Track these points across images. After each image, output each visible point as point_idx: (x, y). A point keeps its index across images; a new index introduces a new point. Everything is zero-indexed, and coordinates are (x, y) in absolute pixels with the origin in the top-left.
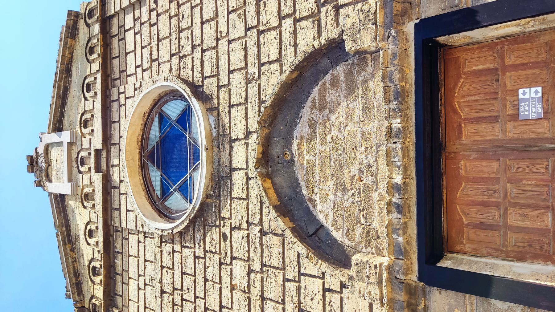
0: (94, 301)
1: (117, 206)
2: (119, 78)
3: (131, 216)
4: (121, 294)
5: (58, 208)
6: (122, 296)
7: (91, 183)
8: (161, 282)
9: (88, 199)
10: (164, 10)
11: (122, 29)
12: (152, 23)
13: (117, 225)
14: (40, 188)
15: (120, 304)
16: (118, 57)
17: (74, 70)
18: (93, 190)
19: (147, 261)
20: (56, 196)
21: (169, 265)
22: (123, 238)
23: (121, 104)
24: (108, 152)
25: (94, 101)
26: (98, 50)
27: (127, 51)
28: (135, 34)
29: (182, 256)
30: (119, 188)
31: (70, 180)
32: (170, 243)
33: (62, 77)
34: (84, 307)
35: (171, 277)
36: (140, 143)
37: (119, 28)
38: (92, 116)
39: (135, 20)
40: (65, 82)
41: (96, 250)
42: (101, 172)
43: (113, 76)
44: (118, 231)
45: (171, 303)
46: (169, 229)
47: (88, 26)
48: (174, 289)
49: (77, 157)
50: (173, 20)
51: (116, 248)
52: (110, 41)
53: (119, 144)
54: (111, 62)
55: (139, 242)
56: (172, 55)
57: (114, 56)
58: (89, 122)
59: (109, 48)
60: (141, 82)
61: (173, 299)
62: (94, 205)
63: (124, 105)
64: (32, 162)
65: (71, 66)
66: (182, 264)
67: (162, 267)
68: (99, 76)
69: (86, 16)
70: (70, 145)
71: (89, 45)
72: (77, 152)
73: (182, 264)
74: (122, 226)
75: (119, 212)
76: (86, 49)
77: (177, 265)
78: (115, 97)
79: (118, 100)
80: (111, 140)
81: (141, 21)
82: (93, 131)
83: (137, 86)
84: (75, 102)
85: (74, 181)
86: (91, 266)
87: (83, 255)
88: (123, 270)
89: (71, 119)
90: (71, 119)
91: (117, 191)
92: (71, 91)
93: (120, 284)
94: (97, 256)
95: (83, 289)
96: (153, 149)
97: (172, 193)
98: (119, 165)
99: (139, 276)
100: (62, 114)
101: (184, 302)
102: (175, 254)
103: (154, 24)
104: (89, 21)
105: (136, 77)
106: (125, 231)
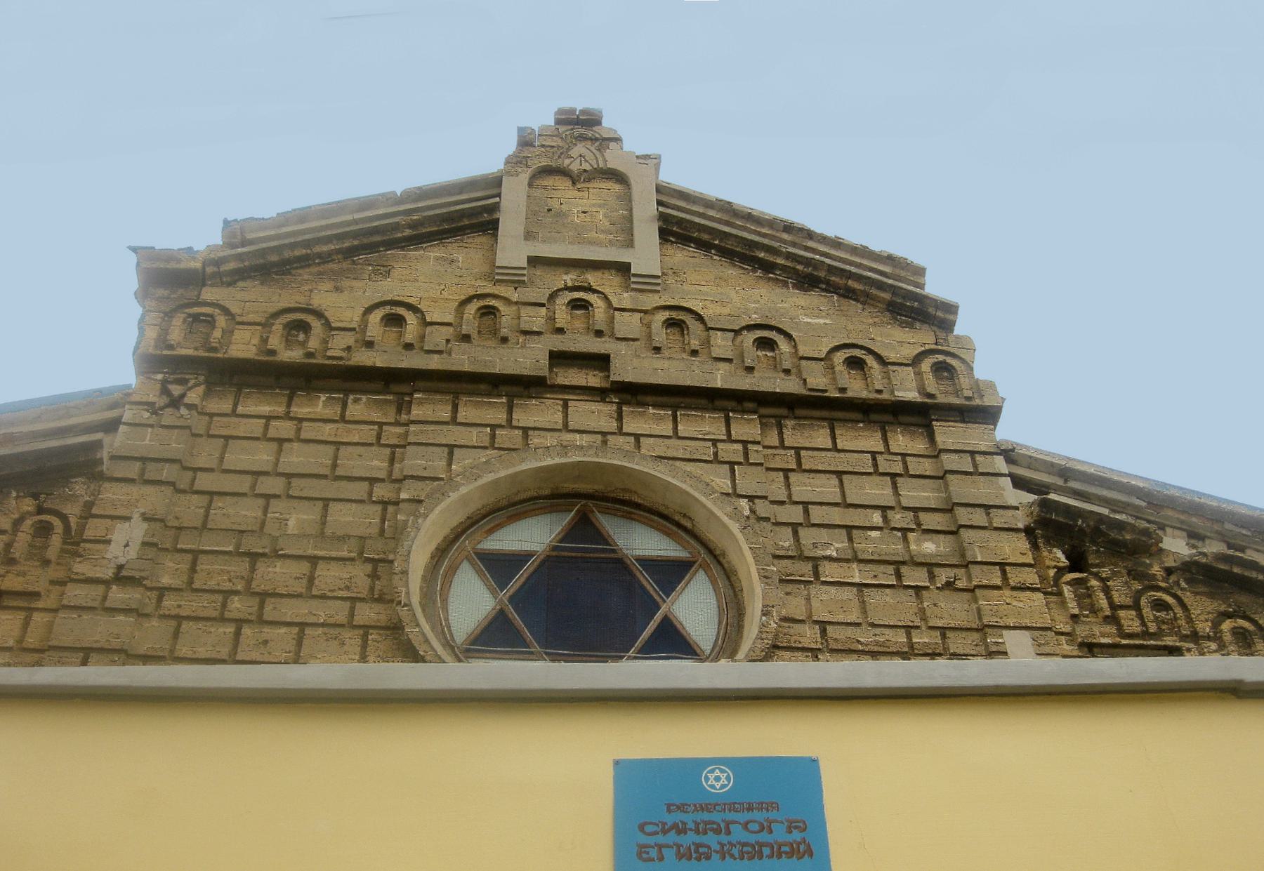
0: (221, 321)
1: (463, 415)
2: (782, 446)
3: (438, 464)
4: (240, 409)
5: (462, 214)
6: (234, 413)
7: (526, 333)
8: (277, 555)
9: (483, 315)
10: (928, 613)
11: (898, 468)
12: (904, 569)
13: (416, 412)
14: (511, 147)
15: (215, 405)
16: (835, 449)
17: (814, 299)
18: (504, 340)
19: (326, 508)
20: (495, 208)
21: (321, 586)
22: (381, 424)
23: (720, 445)
24: (600, 394)
25: (729, 360)
26: (857, 388)
27: (845, 477)
28: (884, 509)
29: (342, 626)
30: (509, 424)
31: (534, 261)
32: (372, 589)
33: (800, 263)
34: (204, 285)
35: (291, 590)
36: (621, 496)
37: (904, 455)
38: (694, 353)
39: (915, 510)
40: (784, 268)
41: (349, 339)
42: (551, 366)
43: (790, 423)
44: (399, 411)
45: (227, 586)
46: (408, 593)
47: (916, 361)
48: (263, 596)
49: (589, 289)
50: (901, 637)
51: (356, 401)
52: (874, 422)
53: (620, 432)
54: (824, 419)
55: (373, 481)
56: (823, 625)
57: (837, 432)
58: (678, 337)
59: (859, 416)
60: (767, 519)
61: (236, 593)
62: (466, 338)
63: (716, 460)
64: (581, 125)
65: (823, 290)
66: (323, 625)
67: (314, 560)
68: (788, 386)
69: (941, 358)
70: (623, 269)
71: (870, 360)
72: (606, 290)
73: (323, 625)
74: (413, 428)
75: (448, 419)
76: (862, 347)
77: (323, 612)
78: (739, 430)
79: (730, 439)
80: (628, 403)
81: (912, 530)
82: (657, 350)
83: (763, 508)
84: (733, 294)
85: (533, 271)
86: (310, 319)
87: (337, 289)
88: (301, 420)
89: (692, 277)
90: (692, 277)
91: (501, 417)
92: (762, 283)
93: (266, 409)
94: (338, 344)
95: (248, 283)
96: (601, 537)
97: (494, 593)
98: (566, 428)
99: (289, 476)
100: (704, 246)
101: (230, 629)
102: (348, 604)
103: (899, 576)
104: (926, 365)
105: (782, 503)
106: (399, 436)
